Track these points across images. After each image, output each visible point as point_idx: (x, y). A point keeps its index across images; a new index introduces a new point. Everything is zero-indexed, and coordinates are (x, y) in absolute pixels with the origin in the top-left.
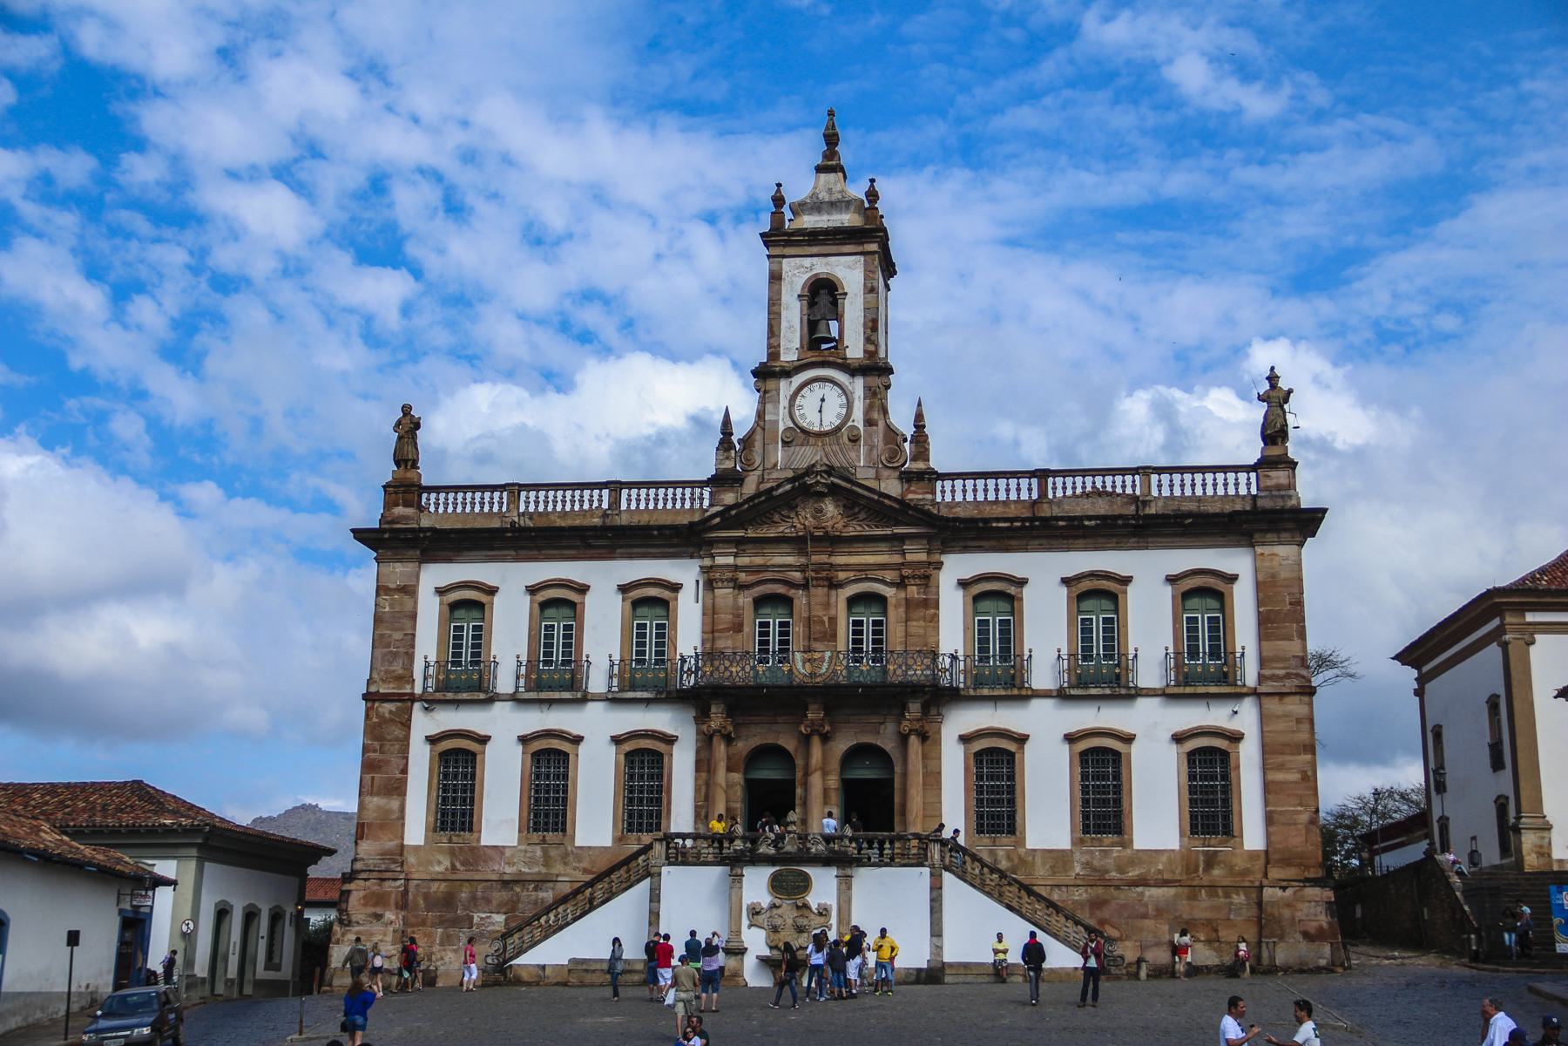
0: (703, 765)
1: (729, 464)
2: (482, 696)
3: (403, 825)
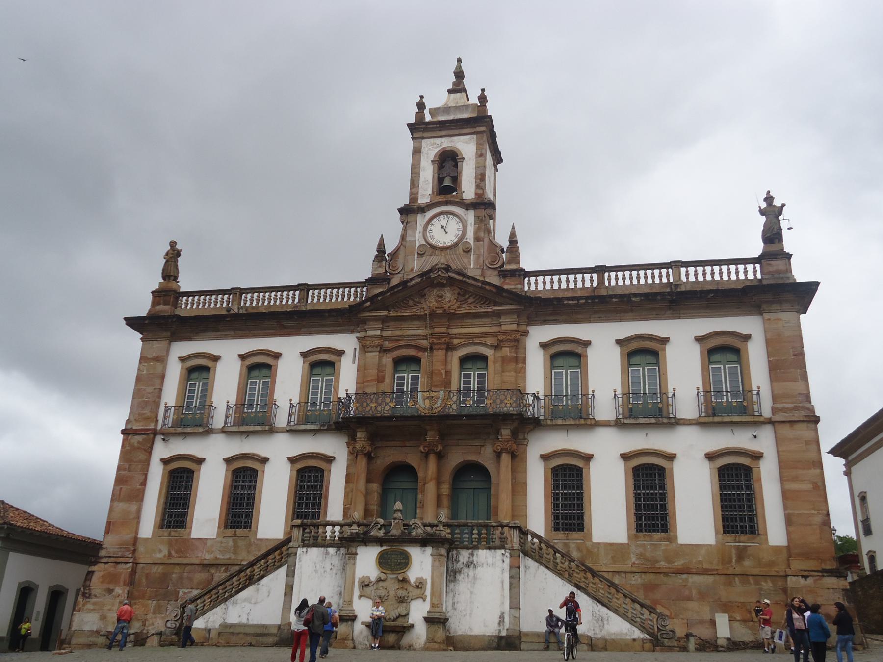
0: (349, 479)
1: (382, 271)
2: (201, 430)
3: (138, 523)
